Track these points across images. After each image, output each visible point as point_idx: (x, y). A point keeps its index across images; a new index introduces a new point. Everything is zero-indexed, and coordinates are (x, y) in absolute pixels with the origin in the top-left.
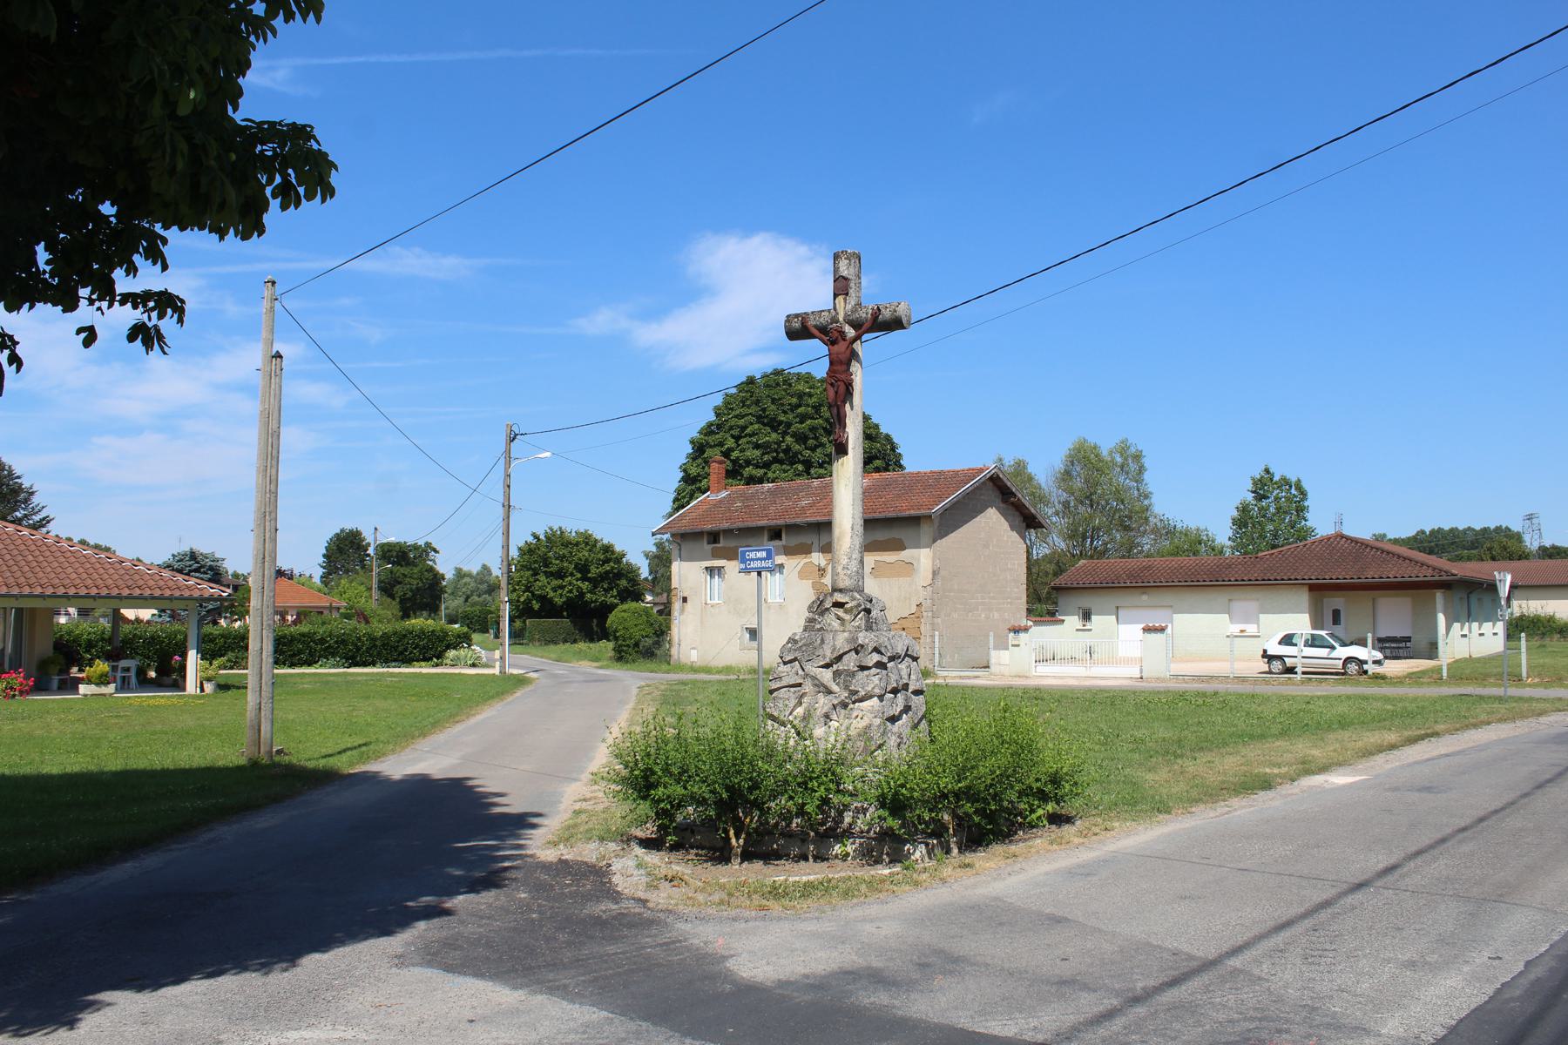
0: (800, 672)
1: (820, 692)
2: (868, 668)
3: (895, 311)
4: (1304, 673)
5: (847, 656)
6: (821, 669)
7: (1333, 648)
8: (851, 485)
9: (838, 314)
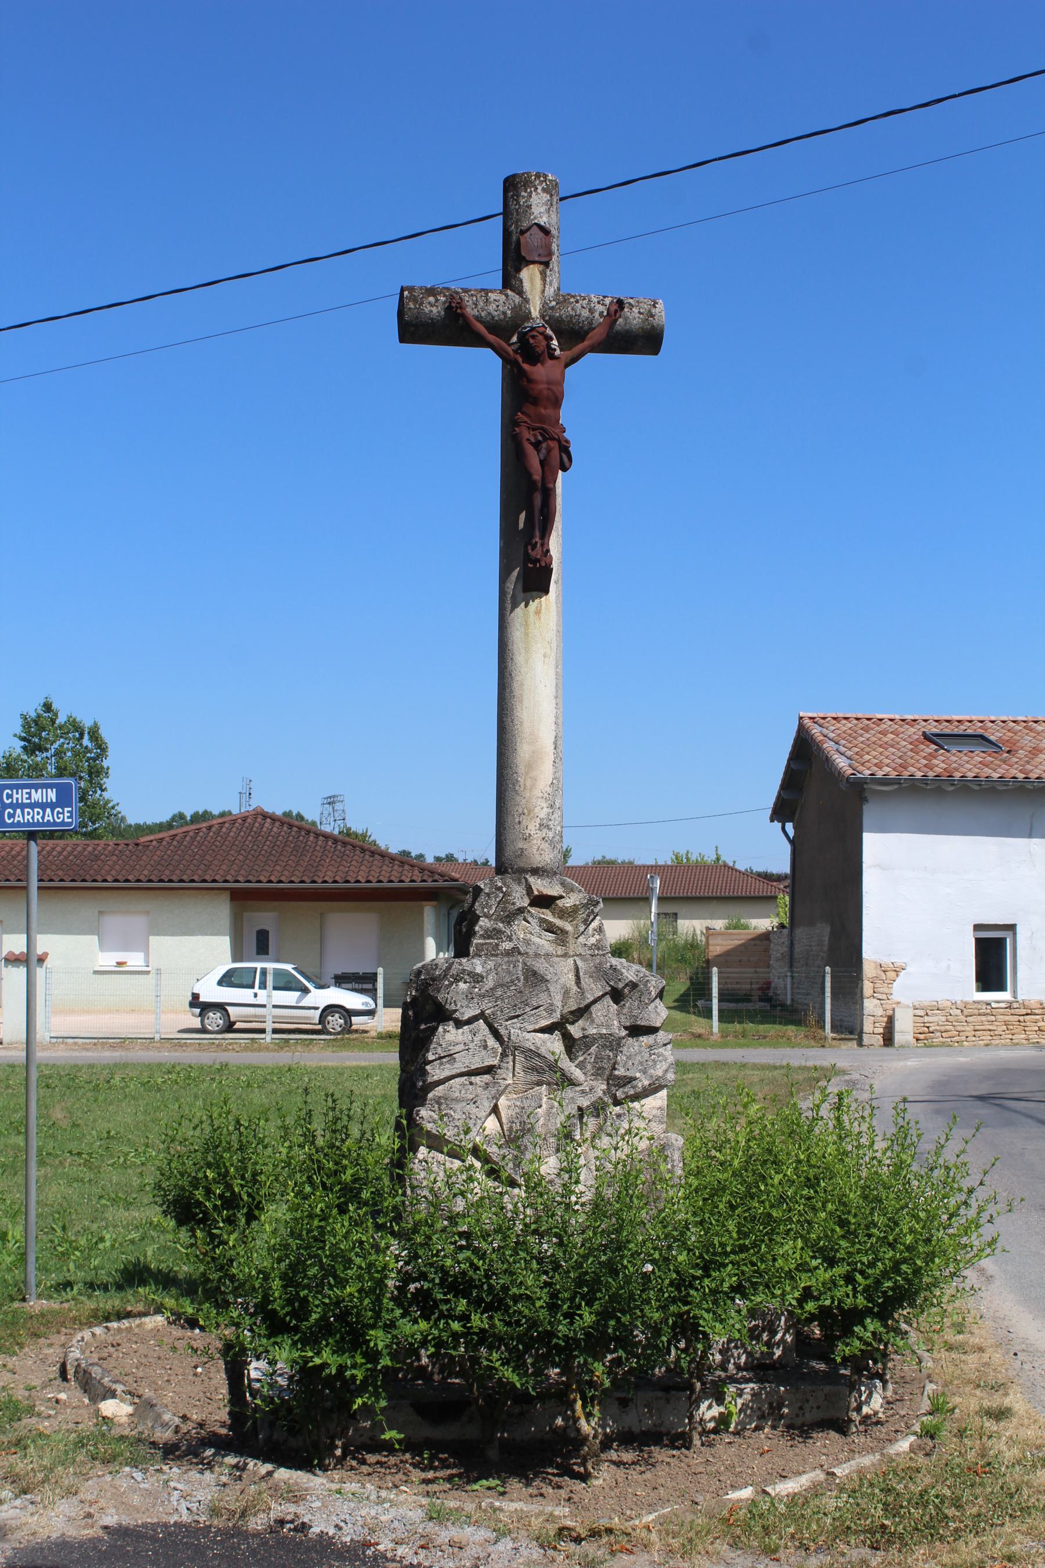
0: (492, 1042)
1: (539, 1084)
2: (652, 1030)
3: (652, 316)
4: (275, 1031)
5: (598, 1006)
6: (539, 1035)
7: (305, 991)
8: (552, 661)
9: (527, 301)
